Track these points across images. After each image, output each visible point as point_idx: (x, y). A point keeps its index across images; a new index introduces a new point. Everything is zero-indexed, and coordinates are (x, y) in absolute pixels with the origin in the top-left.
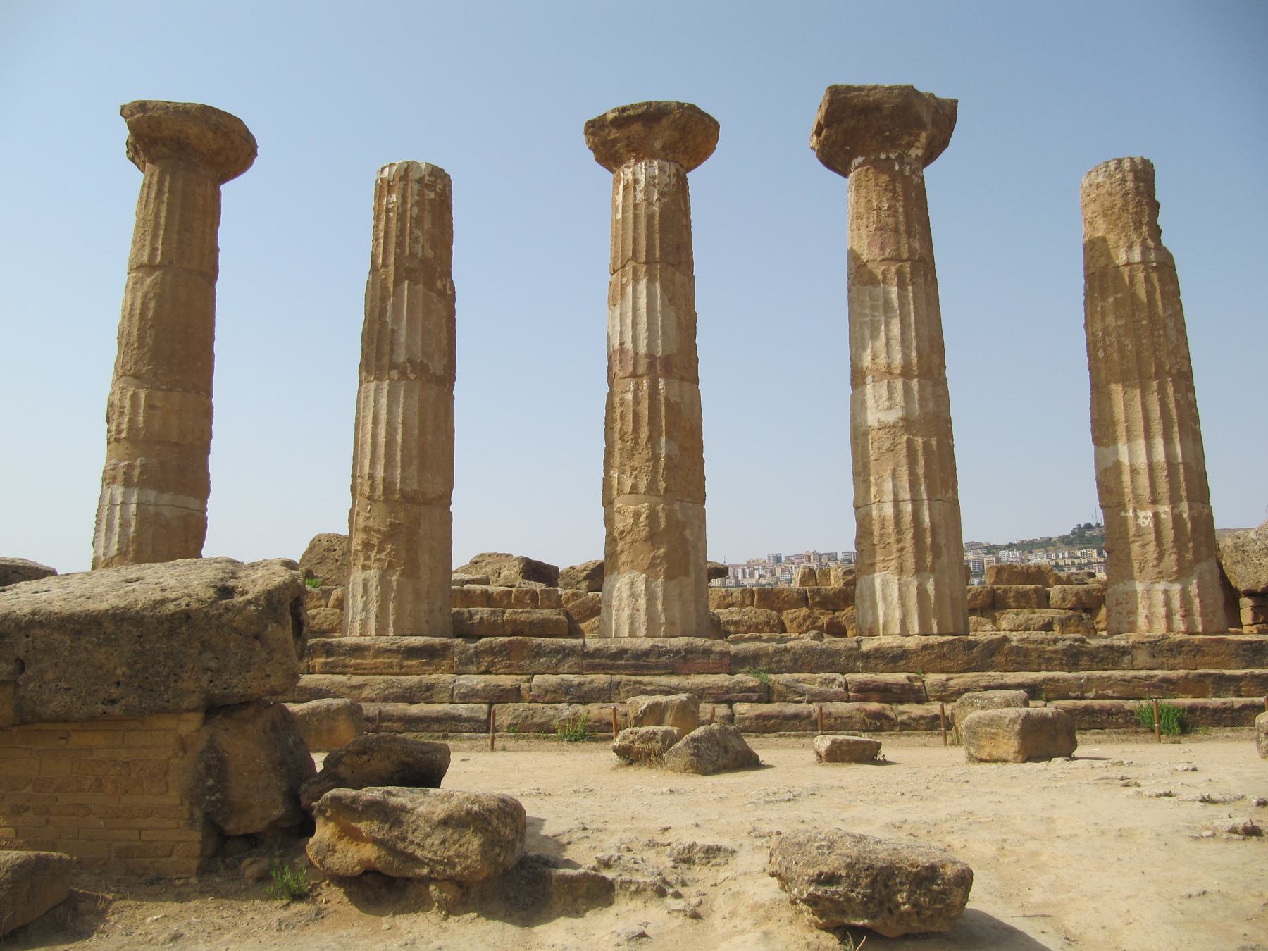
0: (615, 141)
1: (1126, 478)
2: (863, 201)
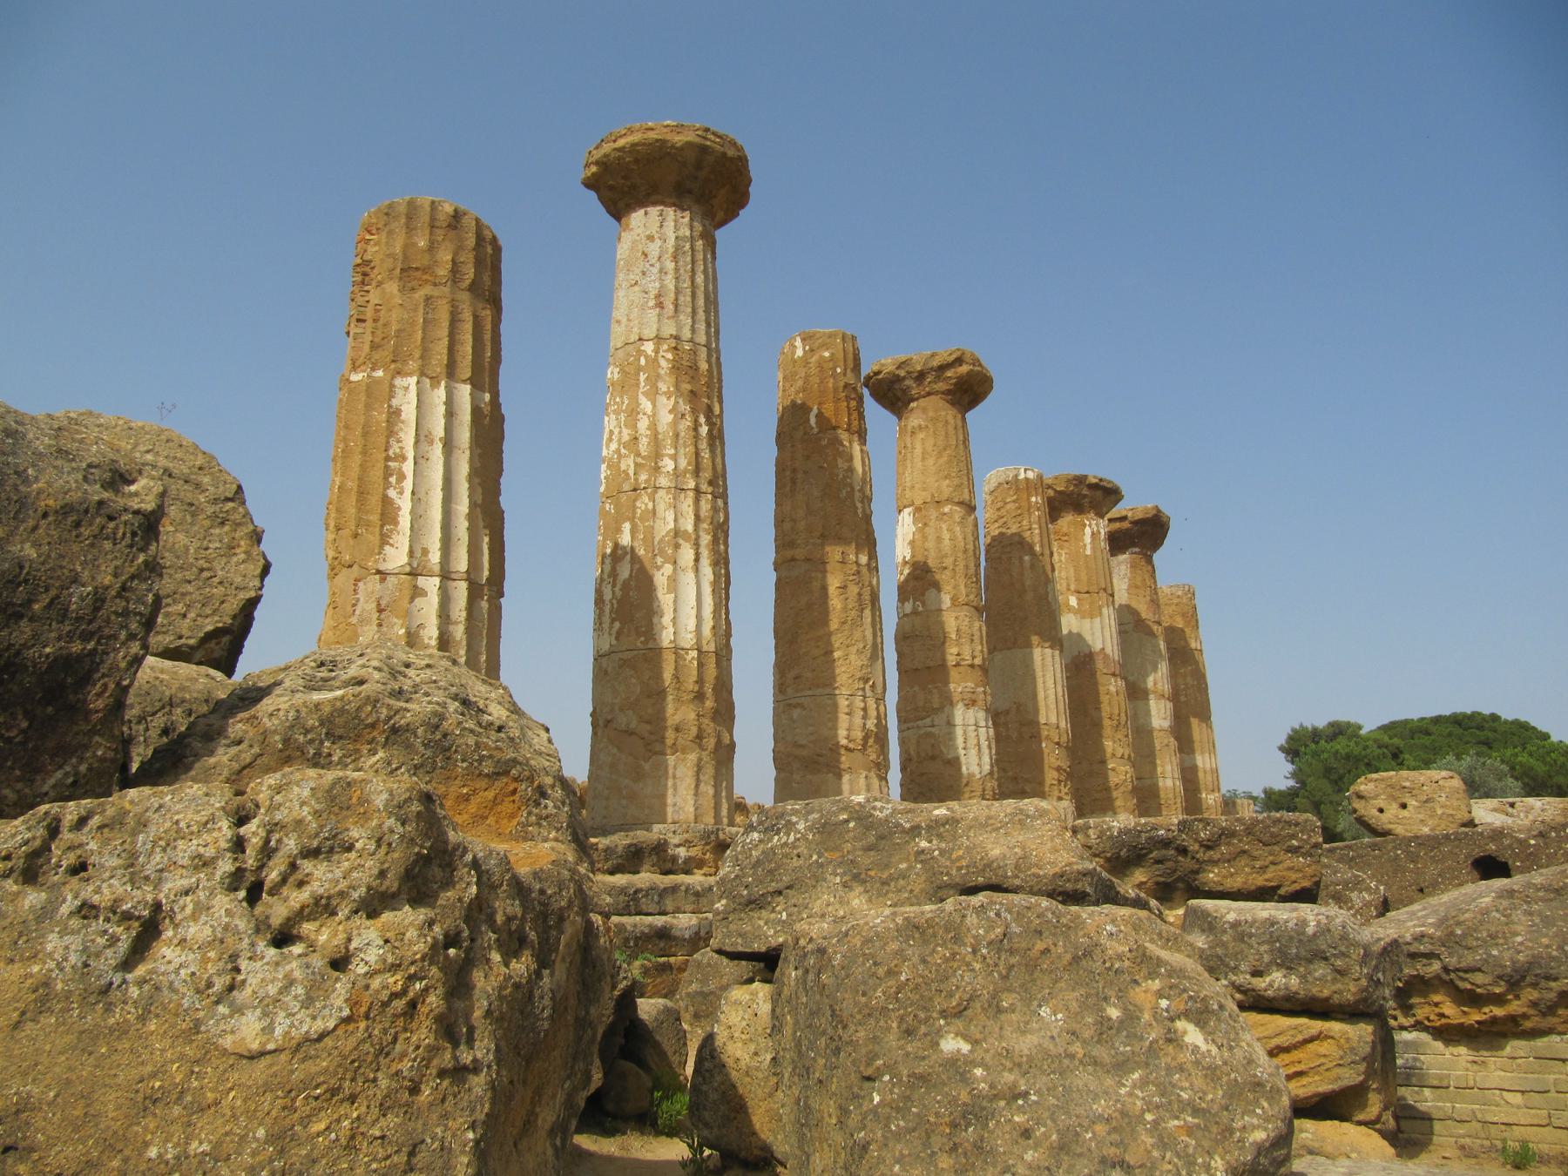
0: (1085, 496)
1: (1201, 775)
2: (1139, 579)
